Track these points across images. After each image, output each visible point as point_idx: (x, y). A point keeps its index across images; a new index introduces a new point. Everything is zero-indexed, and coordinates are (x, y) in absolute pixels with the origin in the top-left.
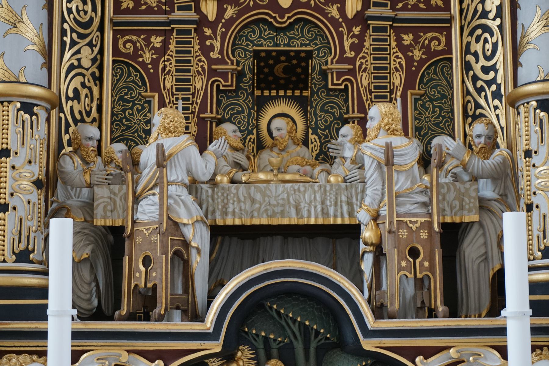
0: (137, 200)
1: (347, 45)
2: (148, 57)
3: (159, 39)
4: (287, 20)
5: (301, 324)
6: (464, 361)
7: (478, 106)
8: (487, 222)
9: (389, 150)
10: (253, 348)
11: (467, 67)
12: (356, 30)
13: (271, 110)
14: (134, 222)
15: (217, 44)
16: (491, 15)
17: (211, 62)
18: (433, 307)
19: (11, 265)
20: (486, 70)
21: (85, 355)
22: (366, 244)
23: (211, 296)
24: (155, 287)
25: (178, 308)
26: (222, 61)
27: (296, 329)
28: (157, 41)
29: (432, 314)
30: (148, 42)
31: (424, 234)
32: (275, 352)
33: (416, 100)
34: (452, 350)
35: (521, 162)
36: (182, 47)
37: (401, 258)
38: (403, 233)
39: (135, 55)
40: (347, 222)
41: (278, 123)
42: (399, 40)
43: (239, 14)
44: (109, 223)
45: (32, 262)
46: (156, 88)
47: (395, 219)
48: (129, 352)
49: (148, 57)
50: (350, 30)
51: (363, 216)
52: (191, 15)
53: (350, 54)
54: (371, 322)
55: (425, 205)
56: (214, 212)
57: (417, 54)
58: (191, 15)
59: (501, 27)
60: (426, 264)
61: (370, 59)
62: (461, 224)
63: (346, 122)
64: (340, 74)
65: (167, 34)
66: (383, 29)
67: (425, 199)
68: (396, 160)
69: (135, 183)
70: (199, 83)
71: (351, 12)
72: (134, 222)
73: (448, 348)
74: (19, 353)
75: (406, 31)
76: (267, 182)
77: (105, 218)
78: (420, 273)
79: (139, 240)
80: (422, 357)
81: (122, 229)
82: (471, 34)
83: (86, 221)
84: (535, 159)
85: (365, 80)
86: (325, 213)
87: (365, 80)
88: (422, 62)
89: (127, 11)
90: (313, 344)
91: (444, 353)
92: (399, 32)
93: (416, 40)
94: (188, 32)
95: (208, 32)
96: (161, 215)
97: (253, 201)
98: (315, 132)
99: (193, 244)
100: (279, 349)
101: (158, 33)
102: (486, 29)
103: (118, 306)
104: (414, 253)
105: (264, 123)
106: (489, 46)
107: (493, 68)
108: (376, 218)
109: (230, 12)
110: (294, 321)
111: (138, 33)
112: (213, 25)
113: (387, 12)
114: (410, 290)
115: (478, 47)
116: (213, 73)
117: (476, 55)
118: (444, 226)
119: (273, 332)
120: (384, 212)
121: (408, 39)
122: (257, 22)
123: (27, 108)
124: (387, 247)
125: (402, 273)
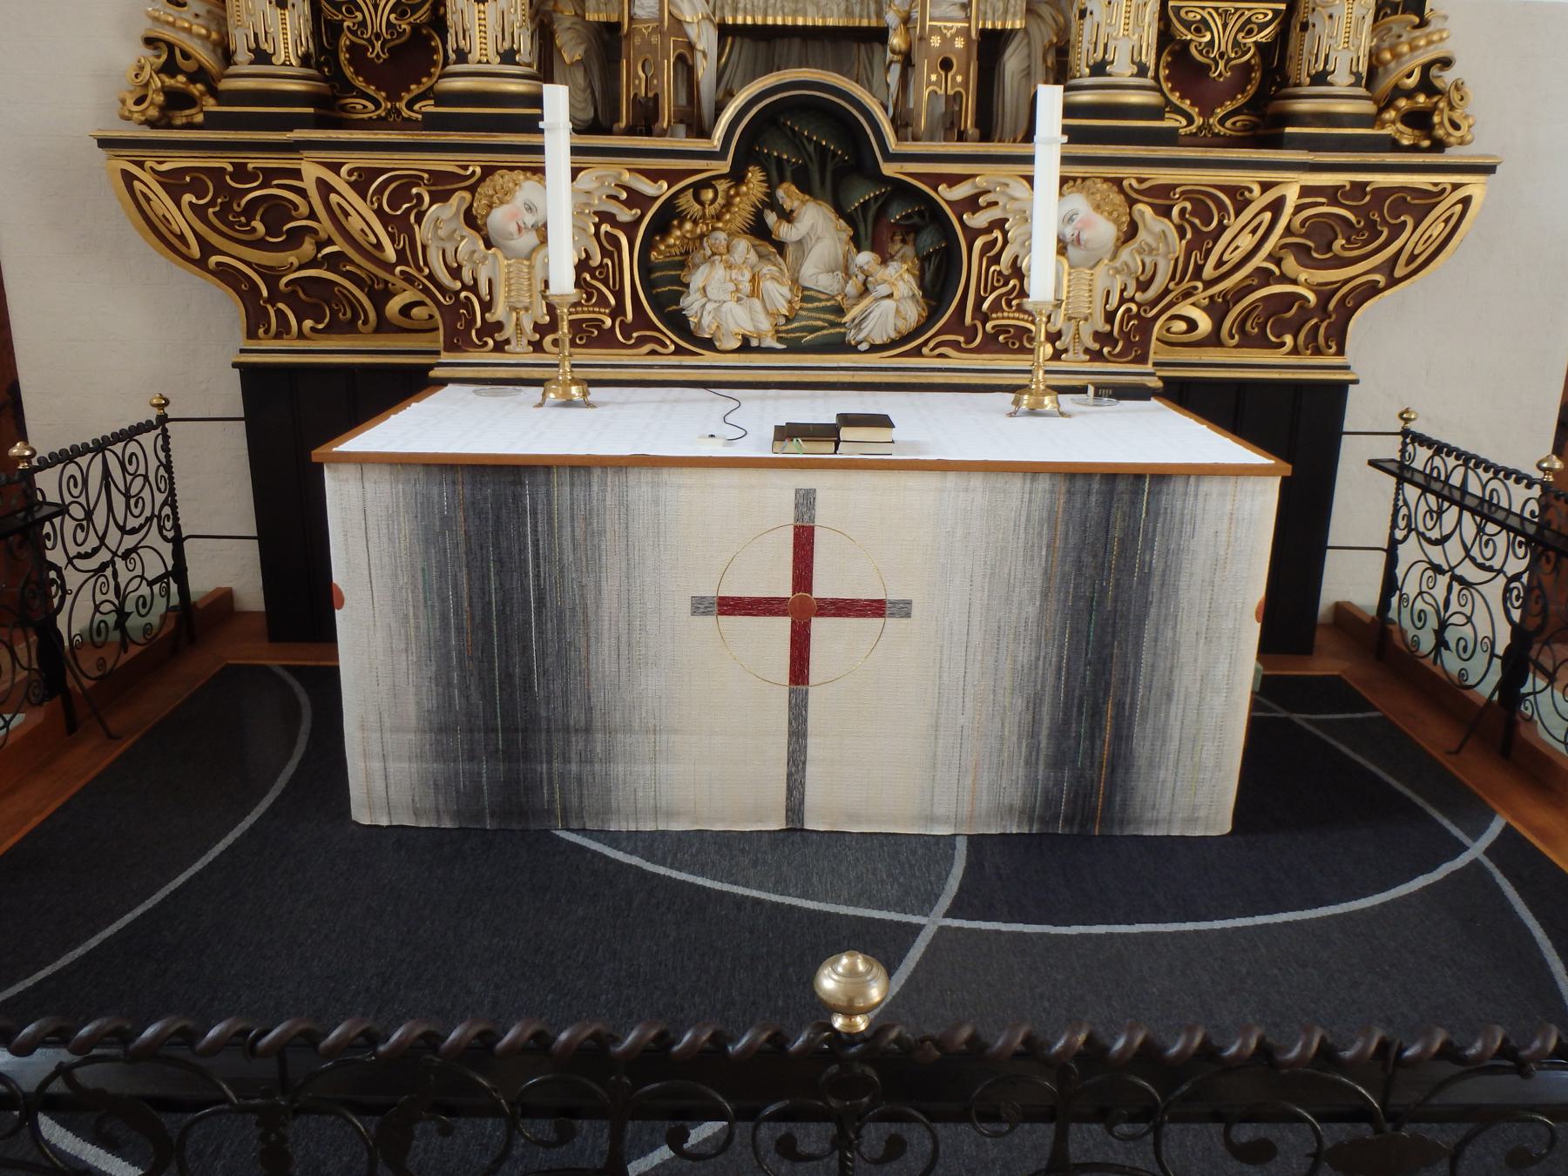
5: (818, 144)
6: (989, 192)
8: (1034, 30)
10: (764, 169)
18: (962, 128)
19: (496, 66)
21: (582, 173)
22: (893, 52)
23: (719, 109)
24: (656, 96)
25: (681, 122)
27: (811, 148)
29: (962, 137)
31: (959, 43)
32: (788, 174)
34: (978, 179)
40: (874, 23)
44: (603, 18)
45: (518, 64)
47: (928, 23)
48: (629, 170)
51: (892, 18)
56: (722, 7)
60: (959, 79)
62: (1003, 31)
72: (631, 19)
73: (974, 176)
74: (511, 169)
77: (598, 11)
78: (952, 88)
79: (637, 40)
80: (945, 185)
81: (618, 25)
83: (576, 14)
86: (849, 12)
90: (830, 168)
91: (970, 181)
96: (661, 10)
99: (700, 46)
100: (792, 171)
103: (618, 120)
104: (946, 65)
110: (809, 139)
118: (983, 33)
119: (787, 153)
125: (931, 88)
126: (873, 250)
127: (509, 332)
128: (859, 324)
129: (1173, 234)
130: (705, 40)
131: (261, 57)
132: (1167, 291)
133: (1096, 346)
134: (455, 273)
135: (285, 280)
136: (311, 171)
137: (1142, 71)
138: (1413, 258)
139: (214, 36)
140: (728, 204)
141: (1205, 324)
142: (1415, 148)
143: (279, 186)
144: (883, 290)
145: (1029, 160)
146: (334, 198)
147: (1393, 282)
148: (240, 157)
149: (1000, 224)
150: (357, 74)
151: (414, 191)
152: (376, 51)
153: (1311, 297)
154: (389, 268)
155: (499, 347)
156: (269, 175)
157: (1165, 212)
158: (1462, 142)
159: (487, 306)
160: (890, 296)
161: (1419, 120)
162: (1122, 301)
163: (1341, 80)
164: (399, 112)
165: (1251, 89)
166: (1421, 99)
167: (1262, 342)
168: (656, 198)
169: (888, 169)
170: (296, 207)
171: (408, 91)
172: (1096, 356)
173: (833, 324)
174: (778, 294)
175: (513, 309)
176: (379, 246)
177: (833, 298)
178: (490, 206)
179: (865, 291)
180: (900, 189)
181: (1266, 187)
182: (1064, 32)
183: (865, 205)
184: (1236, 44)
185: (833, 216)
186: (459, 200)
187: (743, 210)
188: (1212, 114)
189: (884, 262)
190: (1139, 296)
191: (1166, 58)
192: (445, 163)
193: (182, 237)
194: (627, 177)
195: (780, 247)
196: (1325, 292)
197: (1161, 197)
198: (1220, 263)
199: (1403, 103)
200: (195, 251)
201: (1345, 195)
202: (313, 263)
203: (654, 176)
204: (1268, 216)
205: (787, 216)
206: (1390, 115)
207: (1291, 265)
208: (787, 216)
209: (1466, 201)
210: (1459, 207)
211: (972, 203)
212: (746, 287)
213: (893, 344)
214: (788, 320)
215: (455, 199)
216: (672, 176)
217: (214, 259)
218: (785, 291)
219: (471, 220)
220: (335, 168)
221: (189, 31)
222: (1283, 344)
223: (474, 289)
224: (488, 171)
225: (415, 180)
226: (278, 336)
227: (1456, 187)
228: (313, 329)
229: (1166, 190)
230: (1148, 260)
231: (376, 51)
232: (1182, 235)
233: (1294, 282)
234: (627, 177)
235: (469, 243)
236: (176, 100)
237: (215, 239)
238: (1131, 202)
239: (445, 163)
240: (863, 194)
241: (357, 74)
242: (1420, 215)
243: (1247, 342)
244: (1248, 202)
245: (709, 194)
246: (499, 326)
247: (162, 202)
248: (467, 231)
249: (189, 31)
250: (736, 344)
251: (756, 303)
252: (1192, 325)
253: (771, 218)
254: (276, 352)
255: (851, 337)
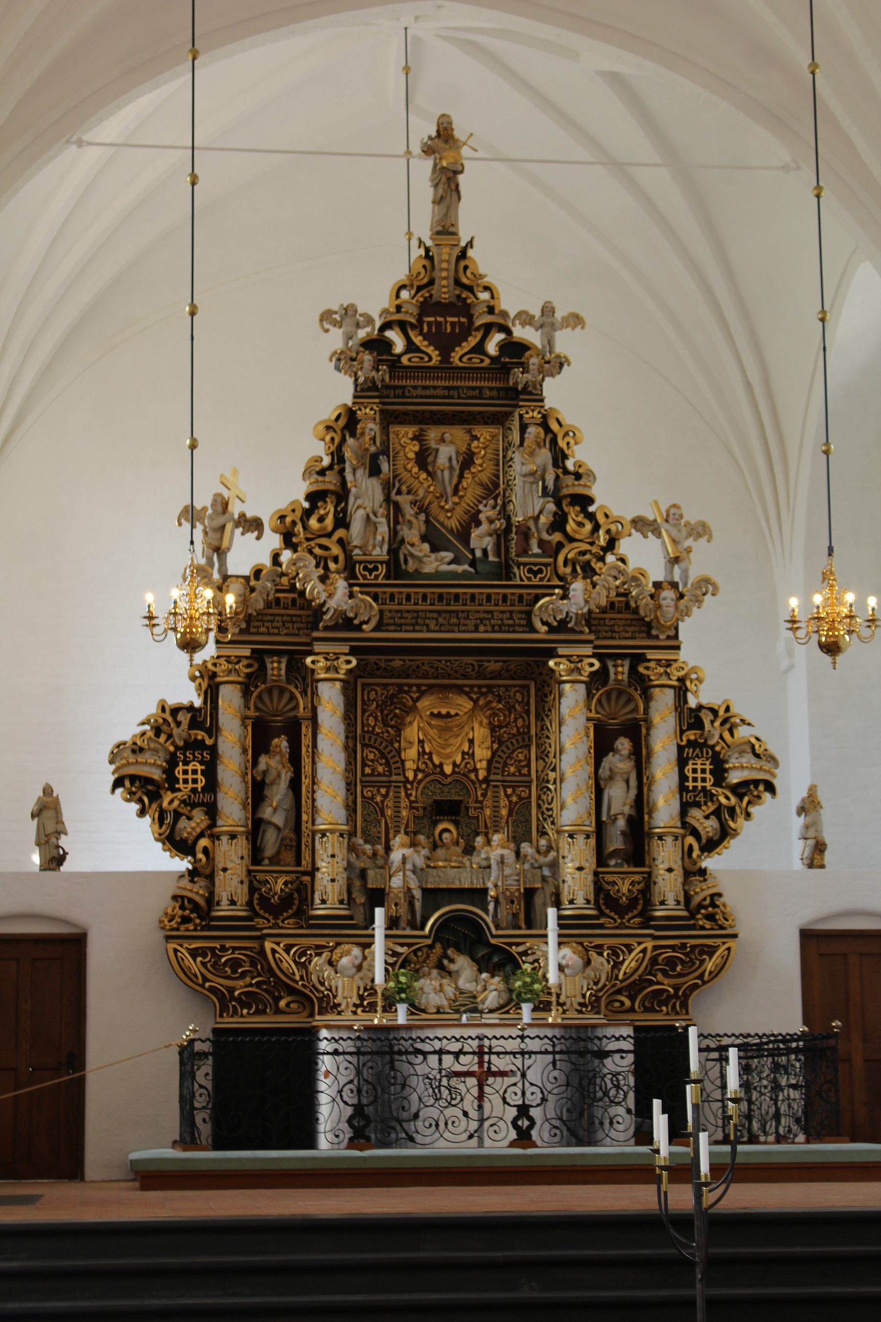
0: (390, 877)
1: (479, 793)
2: (379, 799)
3: (366, 772)
4: (449, 780)
7: (544, 827)
8: (545, 887)
9: (502, 856)
10: (442, 943)
11: (539, 807)
12: (484, 786)
13: (441, 827)
14: (390, 887)
15: (414, 793)
16: (551, 782)
17: (411, 802)
20: (548, 810)
26: (416, 802)
28: (383, 791)
29: (520, 928)
30: (379, 791)
33: (513, 823)
35: (561, 860)
36: (396, 795)
37: (507, 904)
38: (508, 893)
39: (372, 798)
40: (482, 887)
41: (446, 836)
42: (505, 792)
43: (425, 777)
46: (383, 815)
49: (379, 799)
50: (480, 786)
51: (490, 885)
52: (401, 778)
53: (480, 798)
54: (494, 932)
55: (518, 881)
57: (514, 799)
58: (401, 778)
59: (555, 789)
61: (490, 801)
63: (477, 834)
64: (476, 809)
65: (388, 788)
66: (497, 787)
67: (517, 878)
68: (506, 861)
69: (390, 868)
70: (404, 813)
71: (481, 777)
75: (509, 787)
76: (445, 867)
79: (392, 895)
82: (541, 790)
84: (567, 860)
85: (488, 812)
86: (472, 883)
87: (488, 812)
88: (516, 803)
89: (368, 775)
92: (505, 787)
93: (514, 792)
94: (399, 787)
95: (409, 786)
97: (440, 877)
98: (462, 838)
101: (383, 787)
102: (549, 789)
104: (512, 902)
105: (437, 832)
106: (550, 798)
107: (551, 809)
108: (496, 886)
109: (420, 776)
111: (373, 787)
112: (411, 783)
113: (499, 777)
114: (510, 918)
115: (544, 797)
116: (411, 808)
117: (543, 801)
120: (500, 884)
121: (509, 791)
122: (432, 781)
123: (341, 835)
124: (501, 899)
126: (487, 972)
127: (343, 1007)
128: (483, 1002)
129: (605, 962)
130: (417, 894)
131: (233, 902)
132: (605, 985)
133: (579, 1008)
134: (323, 984)
135: (237, 993)
136: (268, 945)
137: (588, 902)
138: (711, 973)
139: (207, 895)
140: (428, 957)
141: (628, 1003)
142: (712, 929)
143: (239, 954)
144: (493, 987)
145: (546, 936)
146: (277, 955)
147: (704, 983)
148: (223, 942)
149: (537, 961)
150: (260, 909)
151: (309, 952)
152: (275, 900)
153: (671, 990)
154: (297, 982)
155: (339, 1013)
156: (234, 949)
157: (601, 954)
158: (731, 927)
159: (335, 997)
160: (496, 990)
161: (711, 917)
162: (588, 989)
163: (671, 902)
164: (278, 924)
165: (640, 907)
166: (710, 909)
167: (651, 1010)
168: (402, 954)
169: (493, 941)
170: (244, 961)
171: (282, 915)
172: (580, 1012)
173: (473, 1003)
174: (450, 990)
175: (345, 998)
176: (294, 974)
177: (471, 992)
178: (341, 957)
179: (485, 989)
180: (497, 949)
181: (639, 943)
182: (557, 888)
183: (483, 956)
184: (629, 890)
185: (469, 960)
186: (326, 955)
187: (434, 958)
188: (624, 918)
189: (493, 976)
190: (595, 988)
191: (602, 896)
192: (321, 941)
193: (195, 975)
194: (391, 945)
195: (450, 973)
196: (676, 988)
197: (599, 949)
198: (625, 973)
199: (703, 911)
200: (200, 981)
201: (680, 948)
202: (251, 985)
203: (402, 945)
204: (641, 955)
205: (452, 961)
206: (699, 916)
207: (660, 977)
208: (452, 961)
209: (729, 949)
210: (726, 952)
211: (525, 953)
212: (438, 988)
213: (497, 1009)
214: (454, 1001)
215: (324, 955)
216: (409, 945)
217: (207, 985)
218: (453, 990)
219: (330, 963)
220: (278, 944)
221: (197, 893)
222: (662, 1011)
223: (330, 990)
224: (338, 944)
225: (309, 948)
226: (232, 1016)
227: (724, 943)
228: (248, 1013)
229: (600, 946)
230: (597, 974)
231: (275, 900)
232: (609, 962)
233: (663, 984)
234: (391, 945)
235: (328, 972)
236: (185, 920)
237: (209, 976)
238: (587, 951)
239: (321, 941)
240: (481, 952)
241: (260, 909)
242: (711, 955)
243: (647, 1010)
244: (633, 950)
245: (420, 954)
246: (339, 1005)
247: (189, 961)
248: (328, 967)
249: (197, 893)
250: (435, 1010)
251: (442, 994)
252: (622, 1003)
253: (445, 962)
254: (229, 1022)
255: (480, 1007)
